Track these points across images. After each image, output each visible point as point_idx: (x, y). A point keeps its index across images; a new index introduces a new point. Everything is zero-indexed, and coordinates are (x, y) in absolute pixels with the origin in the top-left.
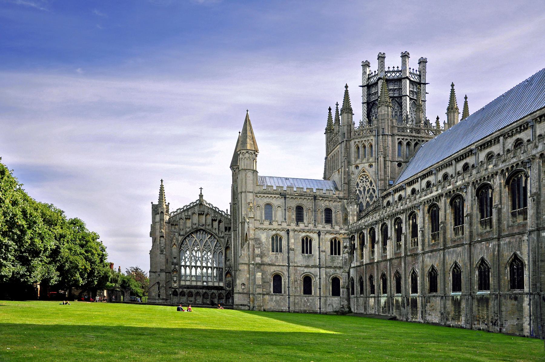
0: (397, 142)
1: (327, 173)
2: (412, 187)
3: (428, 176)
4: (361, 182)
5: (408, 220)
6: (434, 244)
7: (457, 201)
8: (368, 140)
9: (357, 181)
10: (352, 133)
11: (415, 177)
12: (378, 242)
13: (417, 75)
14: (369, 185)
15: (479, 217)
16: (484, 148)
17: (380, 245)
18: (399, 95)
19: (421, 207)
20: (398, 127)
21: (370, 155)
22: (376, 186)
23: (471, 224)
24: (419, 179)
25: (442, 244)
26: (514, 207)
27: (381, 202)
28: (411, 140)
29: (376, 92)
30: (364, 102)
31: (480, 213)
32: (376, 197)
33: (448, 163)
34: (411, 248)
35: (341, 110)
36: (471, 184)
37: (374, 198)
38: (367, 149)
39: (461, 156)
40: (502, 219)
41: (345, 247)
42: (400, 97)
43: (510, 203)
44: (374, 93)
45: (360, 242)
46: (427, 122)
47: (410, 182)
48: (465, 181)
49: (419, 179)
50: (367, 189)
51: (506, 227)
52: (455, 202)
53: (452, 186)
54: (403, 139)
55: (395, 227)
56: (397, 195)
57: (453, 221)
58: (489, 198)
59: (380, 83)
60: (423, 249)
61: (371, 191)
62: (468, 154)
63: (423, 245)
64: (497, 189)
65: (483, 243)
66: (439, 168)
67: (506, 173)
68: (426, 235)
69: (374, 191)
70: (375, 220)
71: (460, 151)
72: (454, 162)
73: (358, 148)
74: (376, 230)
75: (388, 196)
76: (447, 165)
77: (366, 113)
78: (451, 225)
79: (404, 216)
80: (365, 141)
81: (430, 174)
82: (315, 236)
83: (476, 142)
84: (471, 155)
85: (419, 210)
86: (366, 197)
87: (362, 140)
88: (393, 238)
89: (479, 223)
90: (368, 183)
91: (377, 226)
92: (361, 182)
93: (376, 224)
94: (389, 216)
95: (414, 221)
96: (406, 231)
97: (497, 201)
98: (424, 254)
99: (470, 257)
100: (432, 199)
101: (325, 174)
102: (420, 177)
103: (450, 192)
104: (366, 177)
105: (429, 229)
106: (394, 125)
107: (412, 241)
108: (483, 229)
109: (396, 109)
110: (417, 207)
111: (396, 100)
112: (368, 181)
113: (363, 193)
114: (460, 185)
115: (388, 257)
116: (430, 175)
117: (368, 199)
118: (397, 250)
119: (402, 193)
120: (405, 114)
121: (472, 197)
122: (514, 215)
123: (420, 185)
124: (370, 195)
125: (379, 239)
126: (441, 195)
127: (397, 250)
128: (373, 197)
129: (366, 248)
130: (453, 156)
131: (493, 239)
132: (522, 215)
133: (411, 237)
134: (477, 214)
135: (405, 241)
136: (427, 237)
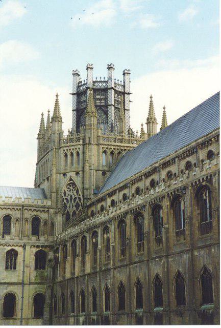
0: (101, 150)
2: (112, 198)
14: (75, 194)
15: (154, 235)
23: (149, 242)
24: (117, 191)
25: (127, 260)
28: (114, 149)
35: (52, 118)
41: (50, 261)
42: (107, 106)
46: (130, 132)
50: (73, 198)
54: (107, 148)
56: (99, 206)
59: (88, 92)
60: (114, 264)
61: (77, 199)
63: (114, 260)
68: (117, 249)
69: (79, 198)
72: (143, 177)
78: (135, 241)
80: (73, 149)
81: (125, 187)
82: (19, 250)
98: (115, 269)
110: (110, 221)
117: (75, 208)
119: (103, 203)
122: (178, 234)
126: (126, 213)
134: (153, 232)
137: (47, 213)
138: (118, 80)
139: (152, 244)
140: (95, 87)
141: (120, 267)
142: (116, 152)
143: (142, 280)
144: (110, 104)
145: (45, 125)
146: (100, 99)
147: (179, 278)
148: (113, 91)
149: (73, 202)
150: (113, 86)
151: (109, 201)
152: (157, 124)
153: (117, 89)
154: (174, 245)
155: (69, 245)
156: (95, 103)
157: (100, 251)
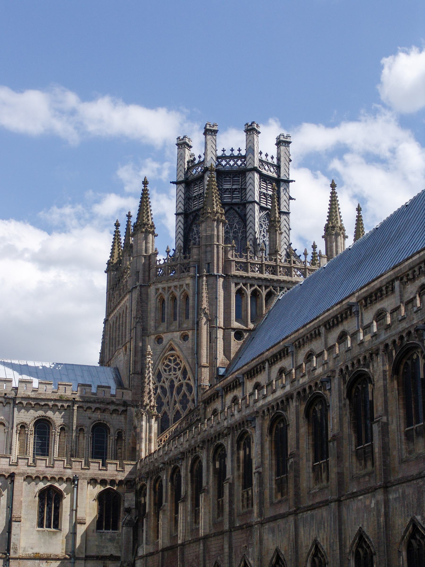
0: (233, 289)
1: (107, 351)
2: (255, 380)
3: (281, 358)
4: (165, 370)
5: (235, 449)
6: (280, 502)
7: (318, 408)
8: (181, 286)
9: (159, 367)
10: (151, 271)
11: (260, 361)
12: (184, 500)
13: (273, 165)
14: (180, 377)
15: (354, 443)
16: (371, 302)
17: (189, 506)
18: (242, 200)
19: (258, 422)
20: (236, 262)
21: (184, 316)
22: (194, 377)
23: (339, 458)
24: (267, 364)
26: (409, 423)
27: (201, 411)
29: (201, 194)
30: (178, 212)
31: (355, 433)
32: (193, 401)
33: (313, 332)
34: (242, 511)
36: (338, 371)
37: (190, 403)
38: (178, 302)
39: (333, 317)
40: (391, 445)
41: (128, 511)
43: (402, 411)
44: (198, 195)
45: (155, 499)
47: (251, 370)
48: (328, 367)
49: (267, 364)
50: (176, 384)
51: (397, 460)
52: (315, 411)
53: (307, 377)
55: (214, 465)
56: (229, 397)
57: (311, 450)
58: (368, 403)
60: (261, 514)
61: (184, 388)
62: (346, 313)
63: (261, 503)
64: (379, 384)
65: (361, 497)
66: (299, 342)
67: (392, 350)
68: (267, 481)
69: (190, 388)
70: (181, 450)
71: (332, 307)
72: (323, 330)
73: (163, 301)
74: (183, 474)
75: (214, 400)
76: (311, 335)
77: (182, 232)
78: (308, 460)
79: (230, 442)
80: (176, 287)
83: (358, 291)
84: (351, 315)
85: (255, 427)
86: (175, 401)
87: (170, 285)
88: (211, 490)
89: (354, 454)
90: (179, 373)
91: (184, 463)
92: (165, 370)
93: (183, 459)
94: (203, 442)
95: (248, 453)
96: (233, 473)
97: (380, 408)
98: (262, 524)
99: (340, 529)
100: (274, 404)
101: (102, 353)
102: (267, 360)
103: (304, 390)
104: (175, 360)
105: (271, 469)
106: (230, 257)
107: (243, 496)
108: (361, 467)
109: (236, 228)
111: (236, 211)
112: (179, 369)
113: (168, 394)
114: (320, 375)
115: (202, 533)
116: (284, 356)
118: (219, 516)
119: (238, 392)
120: (252, 237)
121: (340, 401)
123: (267, 376)
124: (183, 397)
125: (186, 492)
126: (289, 397)
127: (219, 516)
128: (188, 401)
129: (164, 511)
130: (321, 318)
131: (376, 489)
132: (423, 438)
133: (241, 487)
135: (231, 495)
136: (268, 485)
137: (123, 416)
138: (267, 155)
139: (347, 464)
140: (220, 167)
141: (274, 519)
142: (264, 293)
143: (324, 546)
144: (250, 199)
145: (123, 241)
146: (232, 191)
147: (416, 539)
148: (257, 176)
149: (174, 393)
150: (257, 164)
151: (249, 385)
152: (347, 237)
153: (264, 172)
154: (402, 461)
155: (165, 477)
156: (221, 199)
157: (231, 486)
